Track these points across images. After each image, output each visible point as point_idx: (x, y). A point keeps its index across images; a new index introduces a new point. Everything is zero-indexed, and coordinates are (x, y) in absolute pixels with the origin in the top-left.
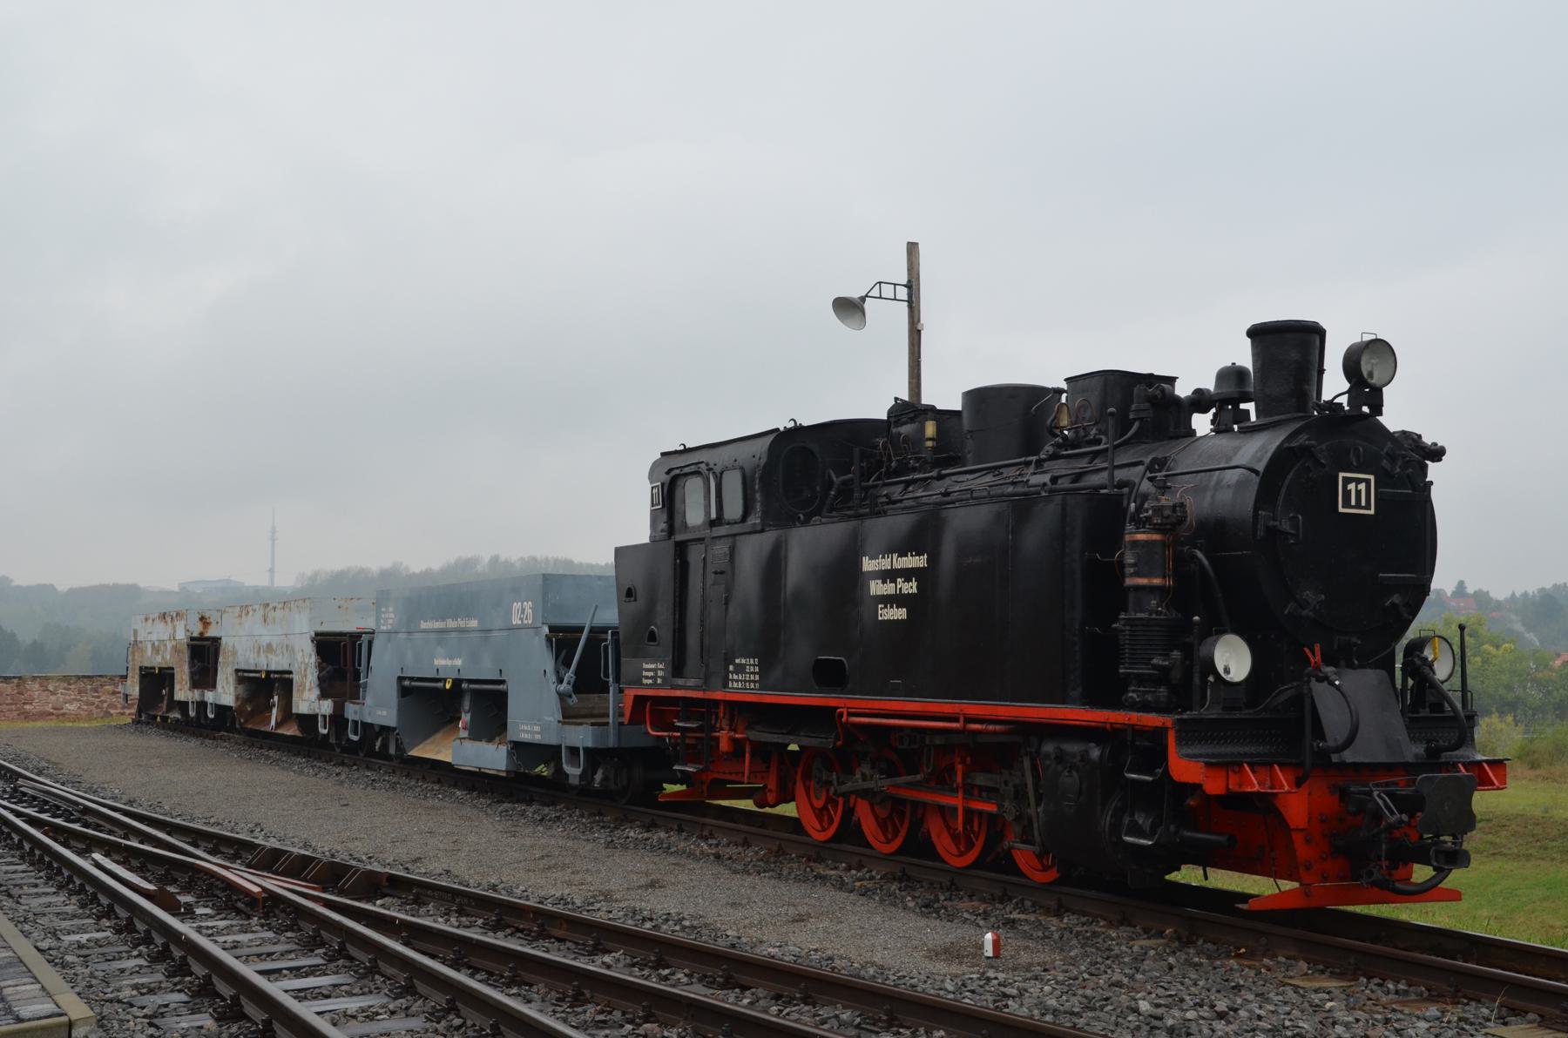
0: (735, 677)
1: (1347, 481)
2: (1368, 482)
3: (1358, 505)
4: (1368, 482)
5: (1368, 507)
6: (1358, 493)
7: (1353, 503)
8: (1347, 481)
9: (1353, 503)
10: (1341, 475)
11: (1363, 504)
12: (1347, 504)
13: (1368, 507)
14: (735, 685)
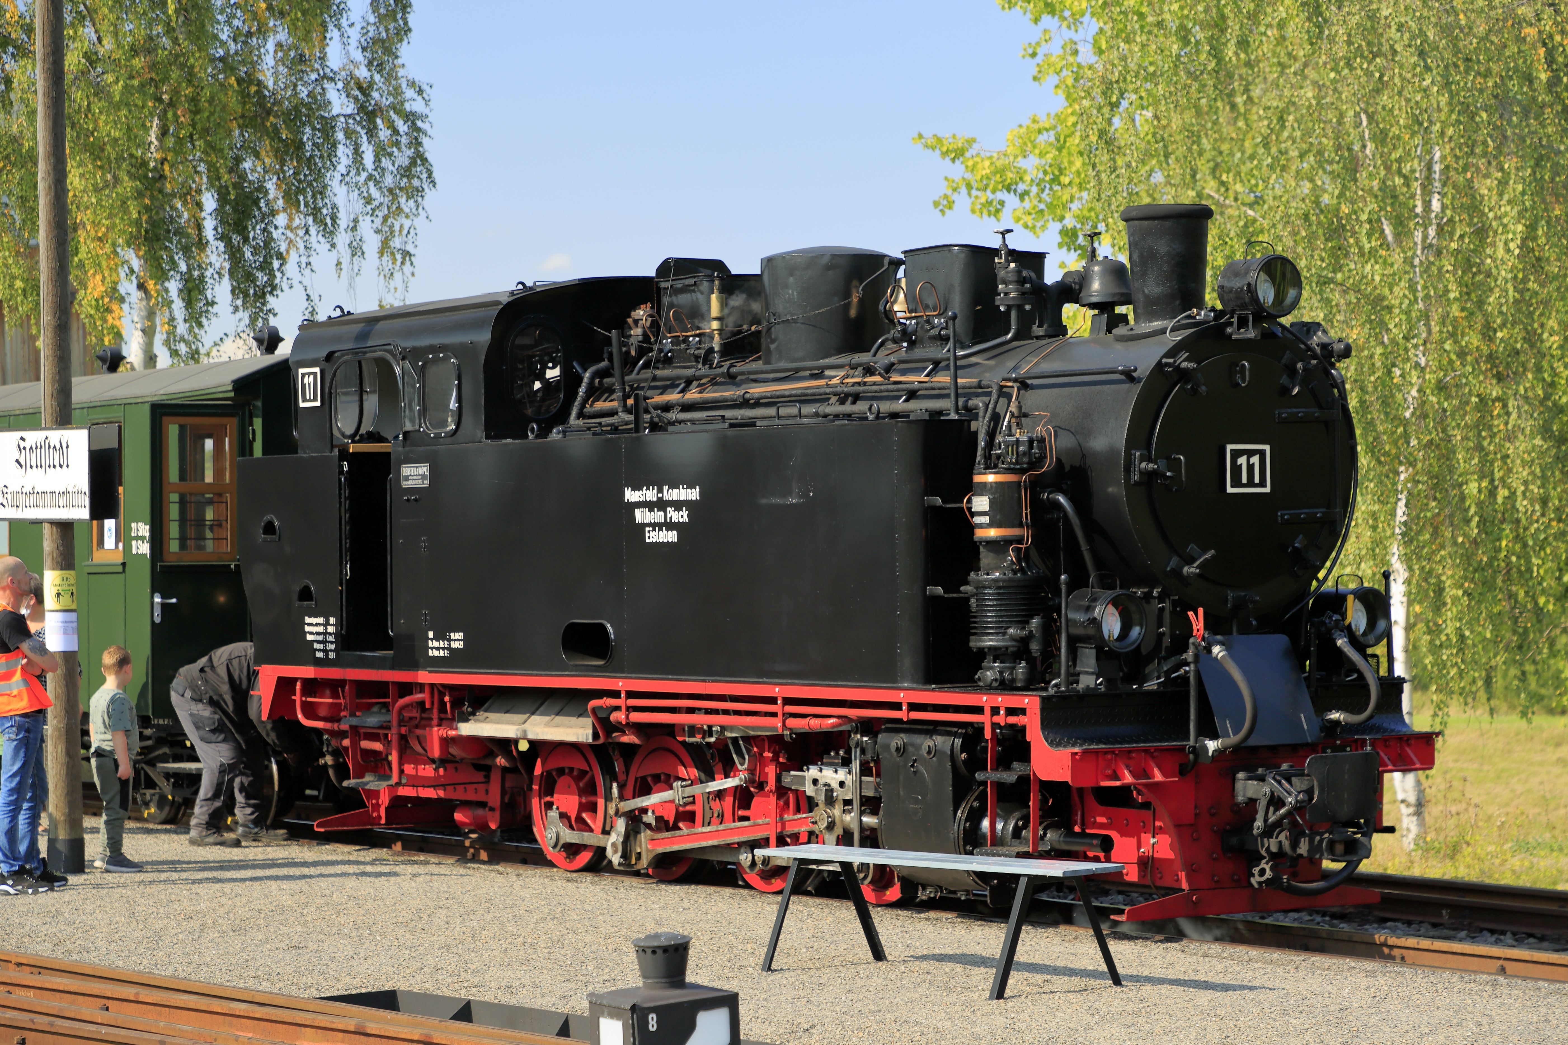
0: (436, 644)
1: (1236, 454)
3: (1251, 483)
4: (1262, 453)
5: (1262, 484)
6: (1250, 468)
7: (1244, 480)
8: (1236, 454)
9: (1244, 480)
10: (1229, 447)
11: (1257, 480)
13: (1262, 484)
14: (436, 653)
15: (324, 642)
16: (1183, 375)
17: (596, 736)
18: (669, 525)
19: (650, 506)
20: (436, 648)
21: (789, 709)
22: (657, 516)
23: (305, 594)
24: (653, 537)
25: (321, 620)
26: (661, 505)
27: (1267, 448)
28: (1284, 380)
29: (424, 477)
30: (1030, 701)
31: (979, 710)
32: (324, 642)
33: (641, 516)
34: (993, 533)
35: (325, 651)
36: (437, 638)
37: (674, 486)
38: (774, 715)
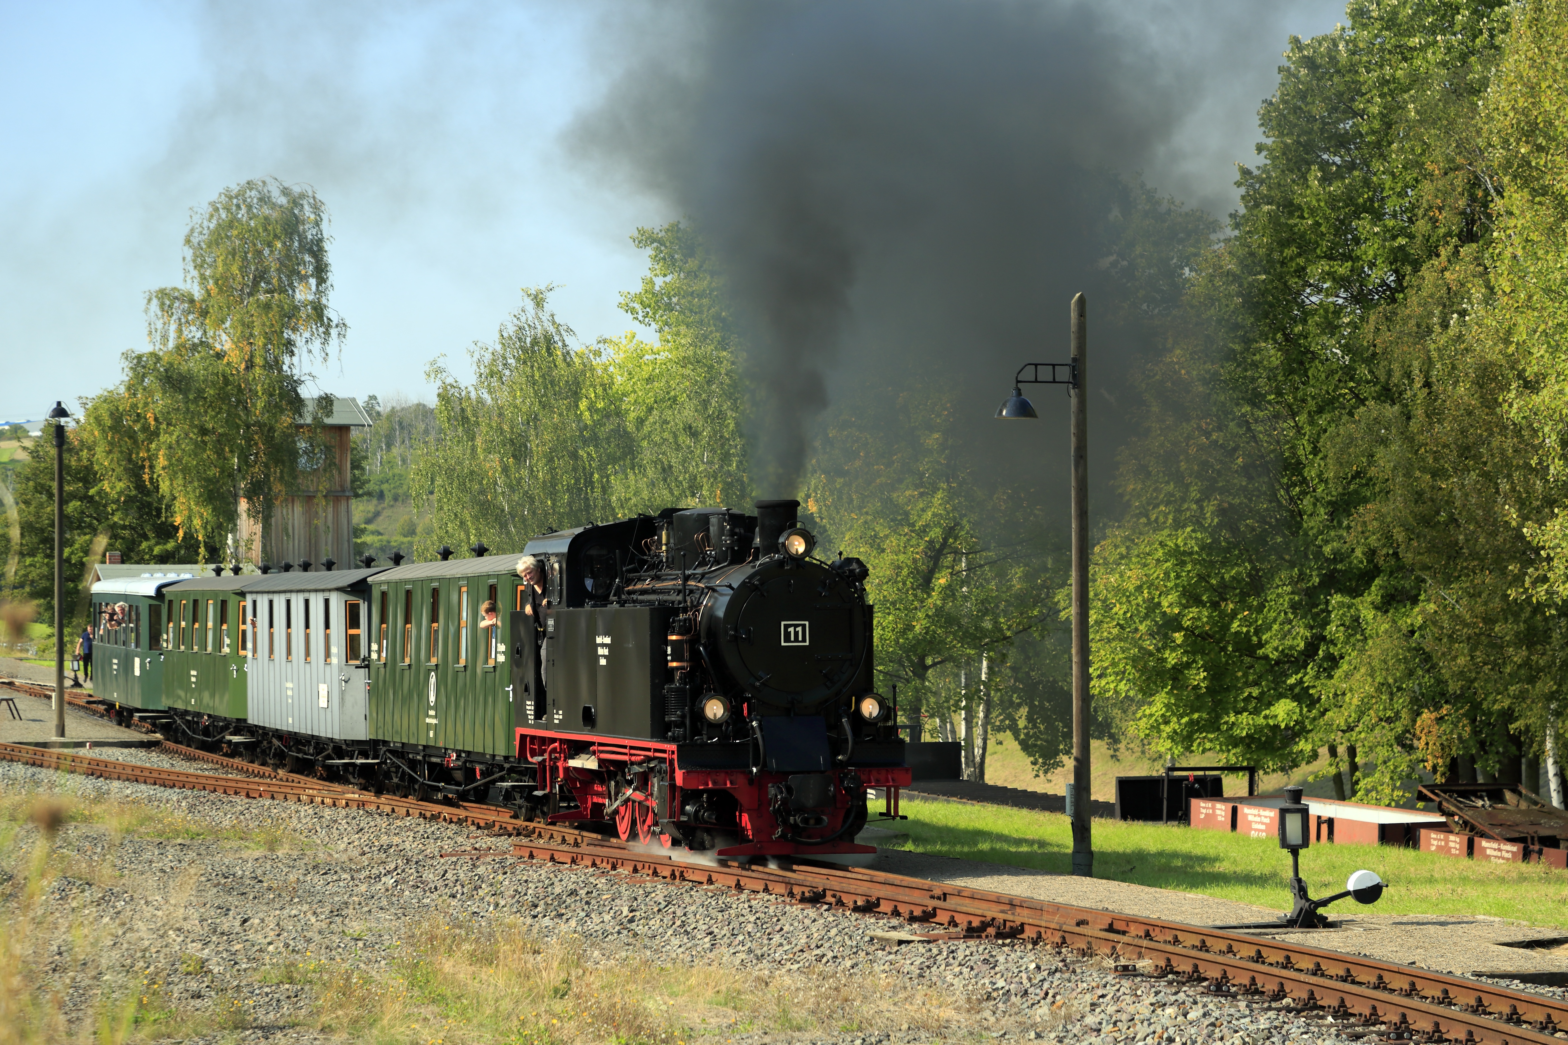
1: (787, 626)
2: (804, 626)
3: (796, 640)
6: (796, 633)
12: (787, 639)
13: (804, 640)
16: (756, 588)
17: (599, 766)
21: (633, 752)
27: (807, 623)
28: (820, 589)
30: (673, 747)
31: (664, 751)
34: (675, 664)
38: (625, 754)
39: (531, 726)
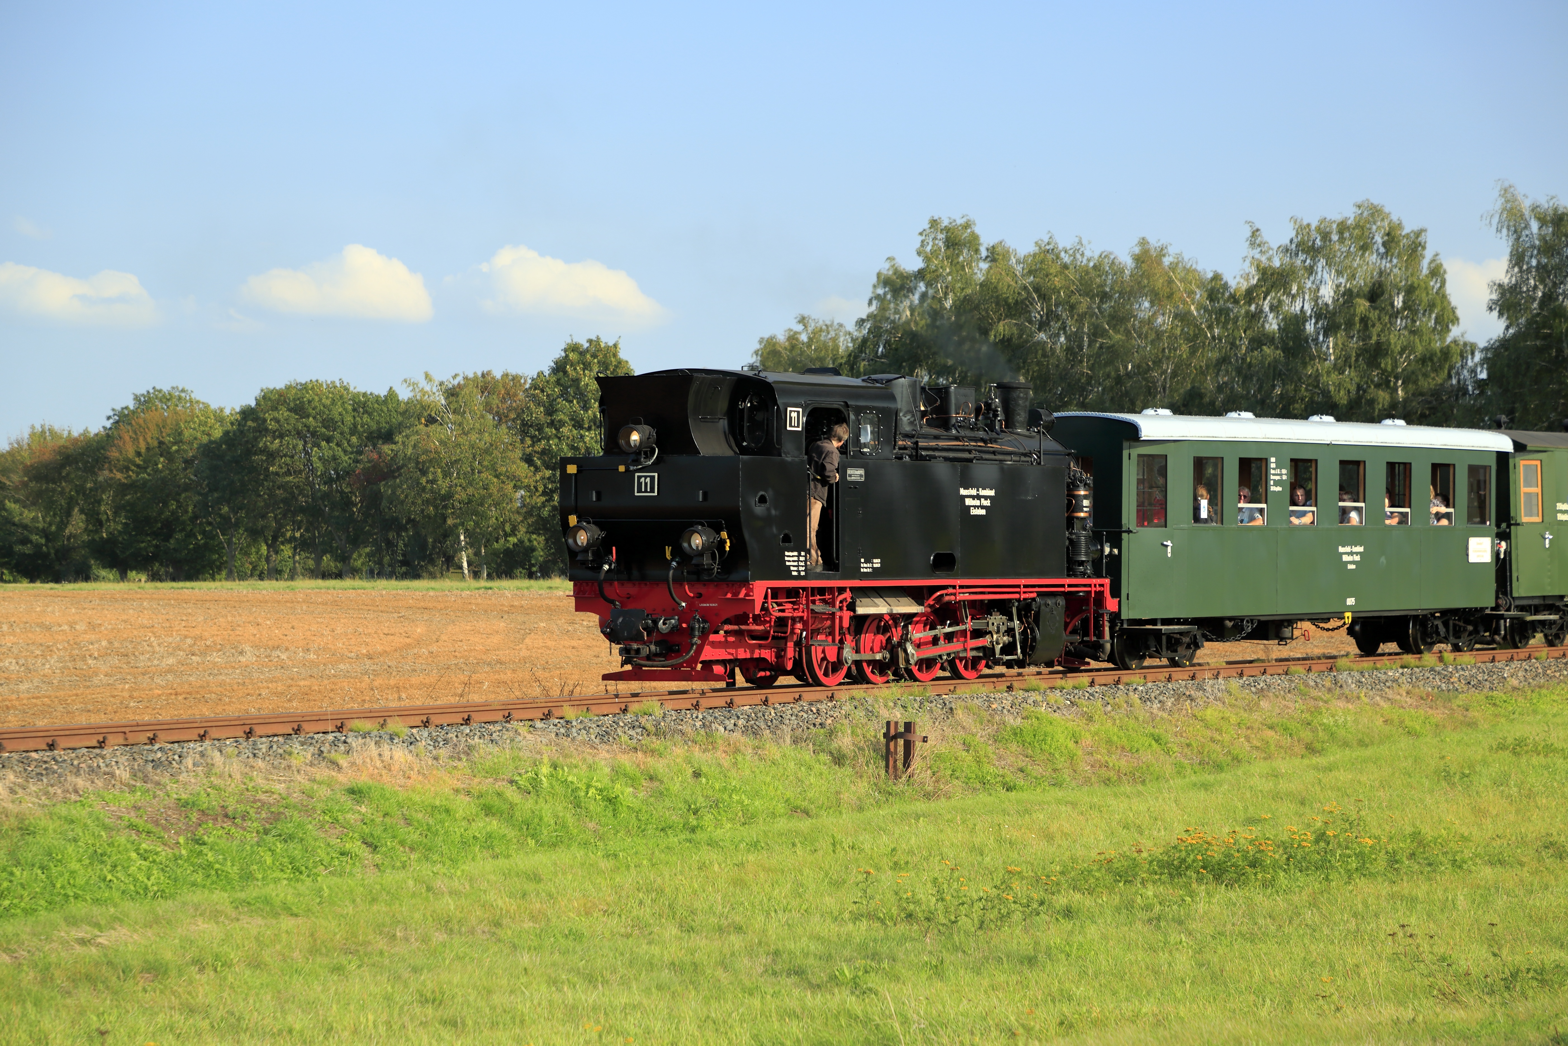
15: (798, 566)
18: (982, 507)
19: (973, 497)
20: (865, 567)
22: (976, 502)
23: (786, 539)
24: (974, 512)
25: (796, 553)
26: (978, 497)
29: (861, 476)
31: (1090, 586)
32: (798, 566)
33: (968, 502)
35: (798, 571)
36: (866, 562)
37: (984, 489)
39: (799, 577)
